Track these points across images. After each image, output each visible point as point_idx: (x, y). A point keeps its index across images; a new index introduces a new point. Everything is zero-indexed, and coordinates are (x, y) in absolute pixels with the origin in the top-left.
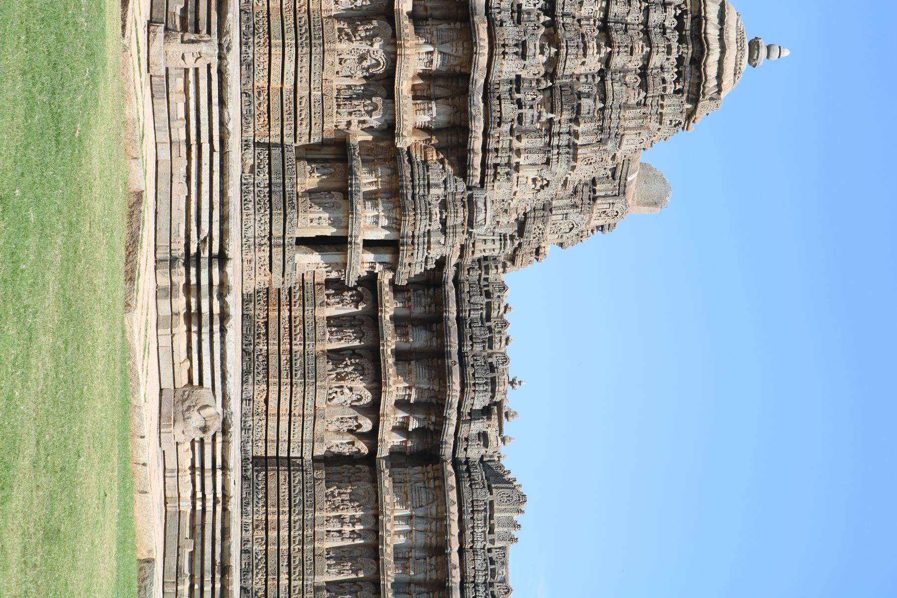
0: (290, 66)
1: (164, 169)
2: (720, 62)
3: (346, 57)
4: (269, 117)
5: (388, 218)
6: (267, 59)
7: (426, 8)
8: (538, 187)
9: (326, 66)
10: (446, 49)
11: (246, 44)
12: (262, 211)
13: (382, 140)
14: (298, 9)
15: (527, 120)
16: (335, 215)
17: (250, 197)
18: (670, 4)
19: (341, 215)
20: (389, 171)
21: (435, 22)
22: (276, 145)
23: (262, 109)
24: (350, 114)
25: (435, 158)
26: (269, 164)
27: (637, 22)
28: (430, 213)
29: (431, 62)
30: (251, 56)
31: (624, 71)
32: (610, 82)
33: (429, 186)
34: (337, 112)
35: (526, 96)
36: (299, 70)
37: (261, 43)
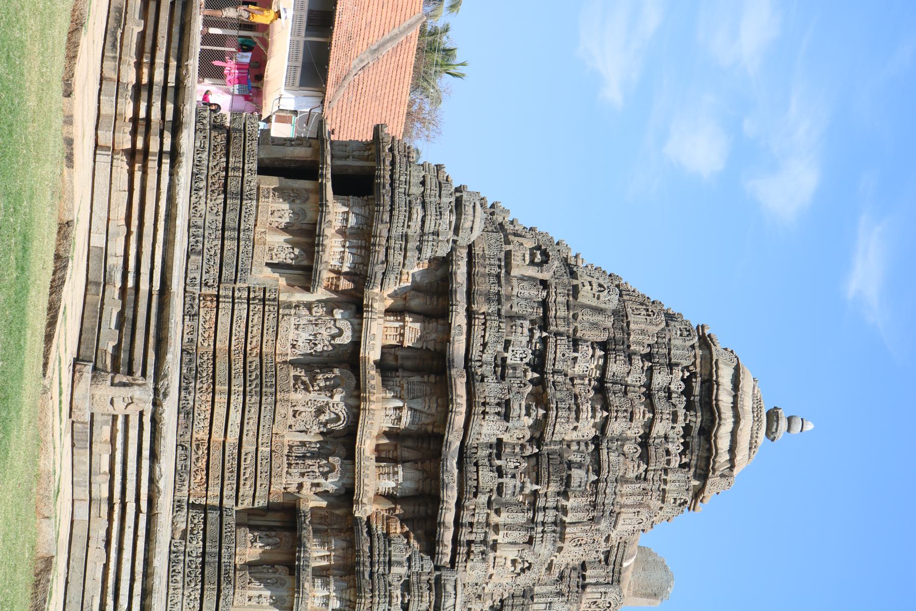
0: (235, 417)
1: (80, 531)
2: (734, 434)
4: (207, 475)
5: (340, 599)
6: (209, 408)
7: (396, 358)
8: (518, 570)
9: (278, 418)
11: (186, 389)
12: (193, 585)
13: (339, 507)
14: (248, 351)
15: (508, 492)
16: (278, 594)
17: (179, 567)
18: (677, 365)
19: (285, 594)
20: (344, 544)
21: (406, 374)
22: (213, 508)
23: (199, 464)
24: (302, 475)
25: (399, 530)
26: (204, 530)
27: (638, 384)
28: (390, 596)
29: (399, 419)
30: (192, 403)
31: (622, 439)
32: (605, 451)
33: (390, 564)
34: (287, 473)
35: (508, 463)
36: (246, 421)
37: (204, 389)
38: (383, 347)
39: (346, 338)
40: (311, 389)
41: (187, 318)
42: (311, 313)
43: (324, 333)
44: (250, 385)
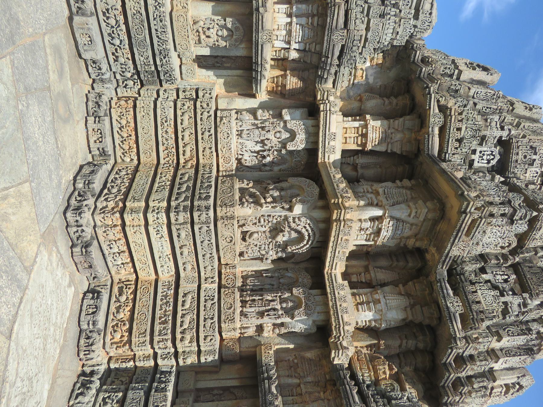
0: (162, 247)
3: (253, 229)
9: (222, 243)
10: (401, 212)
13: (309, 348)
23: (121, 316)
24: (261, 314)
25: (388, 372)
29: (378, 232)
34: (242, 314)
36: (178, 252)
37: (110, 207)
38: (344, 152)
39: (299, 144)
40: (263, 201)
41: (91, 119)
42: (256, 118)
43: (274, 139)
44: (177, 199)
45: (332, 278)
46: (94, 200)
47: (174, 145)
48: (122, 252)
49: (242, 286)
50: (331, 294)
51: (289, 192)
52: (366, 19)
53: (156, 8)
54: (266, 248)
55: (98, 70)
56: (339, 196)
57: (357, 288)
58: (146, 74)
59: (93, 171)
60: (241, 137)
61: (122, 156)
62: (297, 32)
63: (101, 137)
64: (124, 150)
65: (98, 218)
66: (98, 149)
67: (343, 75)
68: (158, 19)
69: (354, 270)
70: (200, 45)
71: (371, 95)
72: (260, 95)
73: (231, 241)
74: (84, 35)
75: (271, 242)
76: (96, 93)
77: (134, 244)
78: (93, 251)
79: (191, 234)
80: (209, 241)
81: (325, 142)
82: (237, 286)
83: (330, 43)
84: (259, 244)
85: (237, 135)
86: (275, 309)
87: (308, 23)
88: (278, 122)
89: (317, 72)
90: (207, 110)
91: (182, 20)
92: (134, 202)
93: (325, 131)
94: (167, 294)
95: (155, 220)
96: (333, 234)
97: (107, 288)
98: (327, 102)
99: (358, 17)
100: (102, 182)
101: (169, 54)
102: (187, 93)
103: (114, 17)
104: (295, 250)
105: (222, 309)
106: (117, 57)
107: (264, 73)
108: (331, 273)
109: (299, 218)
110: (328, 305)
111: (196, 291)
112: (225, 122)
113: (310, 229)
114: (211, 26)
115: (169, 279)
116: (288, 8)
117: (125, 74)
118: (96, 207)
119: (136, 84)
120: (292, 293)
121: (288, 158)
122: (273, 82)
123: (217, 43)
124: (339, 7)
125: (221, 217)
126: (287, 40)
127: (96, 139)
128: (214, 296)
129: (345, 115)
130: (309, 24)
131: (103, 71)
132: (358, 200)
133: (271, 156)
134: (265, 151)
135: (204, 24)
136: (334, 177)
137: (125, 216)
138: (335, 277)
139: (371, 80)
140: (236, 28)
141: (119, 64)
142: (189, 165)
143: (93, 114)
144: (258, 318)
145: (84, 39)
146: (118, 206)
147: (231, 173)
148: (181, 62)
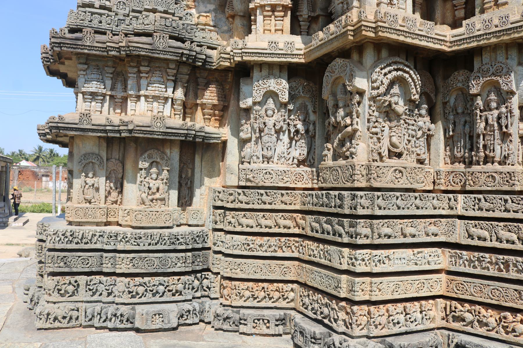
0: (402, 259)
6: (382, 308)
9: (403, 183)
24: (505, 136)
34: (502, 163)
37: (345, 317)
38: (293, 32)
39: (281, 86)
40: (349, 129)
41: (242, 328)
42: (249, 140)
43: (274, 118)
44: (340, 235)
45: (457, 41)
46: (334, 334)
47: (277, 238)
48: (405, 310)
49: (464, 163)
50: (480, 41)
51: (340, 96)
52: (144, 13)
53: (128, 241)
54: (414, 128)
55: (190, 313)
56: (345, 29)
57: (474, 8)
58: (196, 263)
59: (301, 333)
60: (271, 158)
61: (287, 300)
62: (156, 89)
63: (263, 320)
64: (280, 298)
65: (357, 332)
66: (277, 325)
67: (203, 38)
68: (138, 241)
69: (449, 15)
70: (167, 200)
71: (227, 5)
72: (224, 135)
73: (400, 172)
74: (153, 320)
75: (404, 120)
76: (214, 320)
77: (395, 293)
78: (399, 343)
79: (386, 221)
80: (397, 198)
81: (279, 54)
82: (464, 170)
83: (167, 52)
84: (406, 137)
85: (268, 163)
86: (499, 118)
87: (147, 78)
88: (254, 112)
89: (198, 67)
90: (237, 196)
91: (140, 216)
92: (341, 288)
93: (266, 54)
94: (467, 261)
95: (366, 264)
96: (394, 37)
97: (453, 335)
98: (232, 53)
99: (141, 22)
100: (316, 324)
101: (174, 234)
102: (218, 219)
103: (136, 287)
104: (416, 89)
105: (494, 189)
106: (177, 291)
107: (197, 126)
108: (451, 42)
109: (372, 82)
110: (495, 48)
111: (466, 221)
112: (252, 175)
113: (388, 69)
114: (147, 186)
115: (447, 256)
116: (130, 100)
117: (196, 287)
118: (344, 333)
119: (206, 276)
120: (476, 95)
121: (299, 102)
122: (210, 119)
123: (165, 181)
124: (130, 42)
125: (367, 181)
126: (163, 101)
127: (265, 327)
128: (475, 198)
129: (250, 32)
130: (147, 76)
131: (191, 309)
132: (352, 8)
133: (295, 122)
134: (289, 130)
135: (145, 193)
136: (322, 40)
137: (357, 299)
138: (456, 36)
139: (212, 7)
140: (150, 157)
141: (185, 291)
142: (302, 222)
143: (236, 326)
144: (511, 141)
145: (158, 321)
146: (345, 308)
147: (315, 173)
148: (186, 225)
